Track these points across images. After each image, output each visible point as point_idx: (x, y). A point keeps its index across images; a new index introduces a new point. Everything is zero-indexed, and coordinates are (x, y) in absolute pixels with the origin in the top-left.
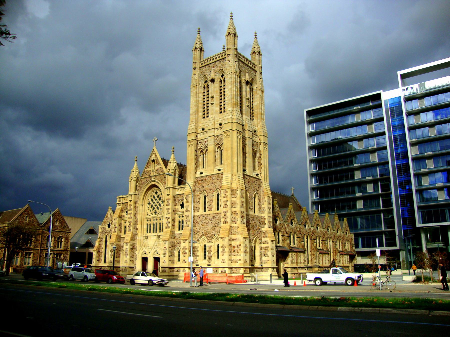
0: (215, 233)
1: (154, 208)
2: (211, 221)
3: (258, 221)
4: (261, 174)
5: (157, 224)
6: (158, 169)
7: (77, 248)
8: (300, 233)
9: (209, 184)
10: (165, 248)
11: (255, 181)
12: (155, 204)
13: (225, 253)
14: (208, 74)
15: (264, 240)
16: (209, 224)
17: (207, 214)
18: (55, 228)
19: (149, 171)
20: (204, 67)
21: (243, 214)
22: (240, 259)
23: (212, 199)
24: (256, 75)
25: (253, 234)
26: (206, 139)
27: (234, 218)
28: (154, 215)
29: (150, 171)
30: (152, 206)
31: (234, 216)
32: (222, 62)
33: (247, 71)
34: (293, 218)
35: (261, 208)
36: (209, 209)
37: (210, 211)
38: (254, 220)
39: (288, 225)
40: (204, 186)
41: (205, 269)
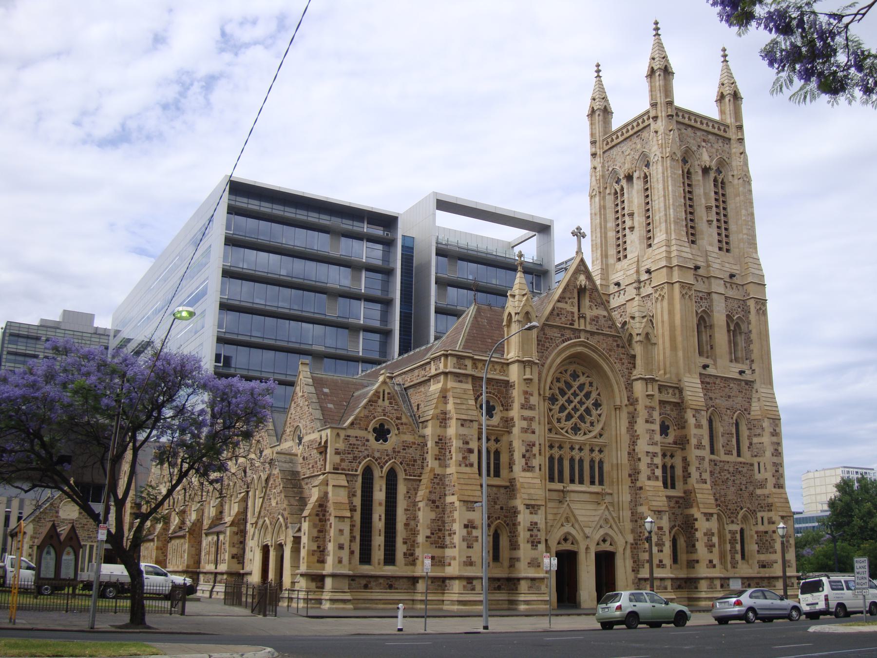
2: (732, 478)
5: (581, 461)
7: (651, 522)
10: (660, 528)
16: (729, 483)
17: (724, 462)
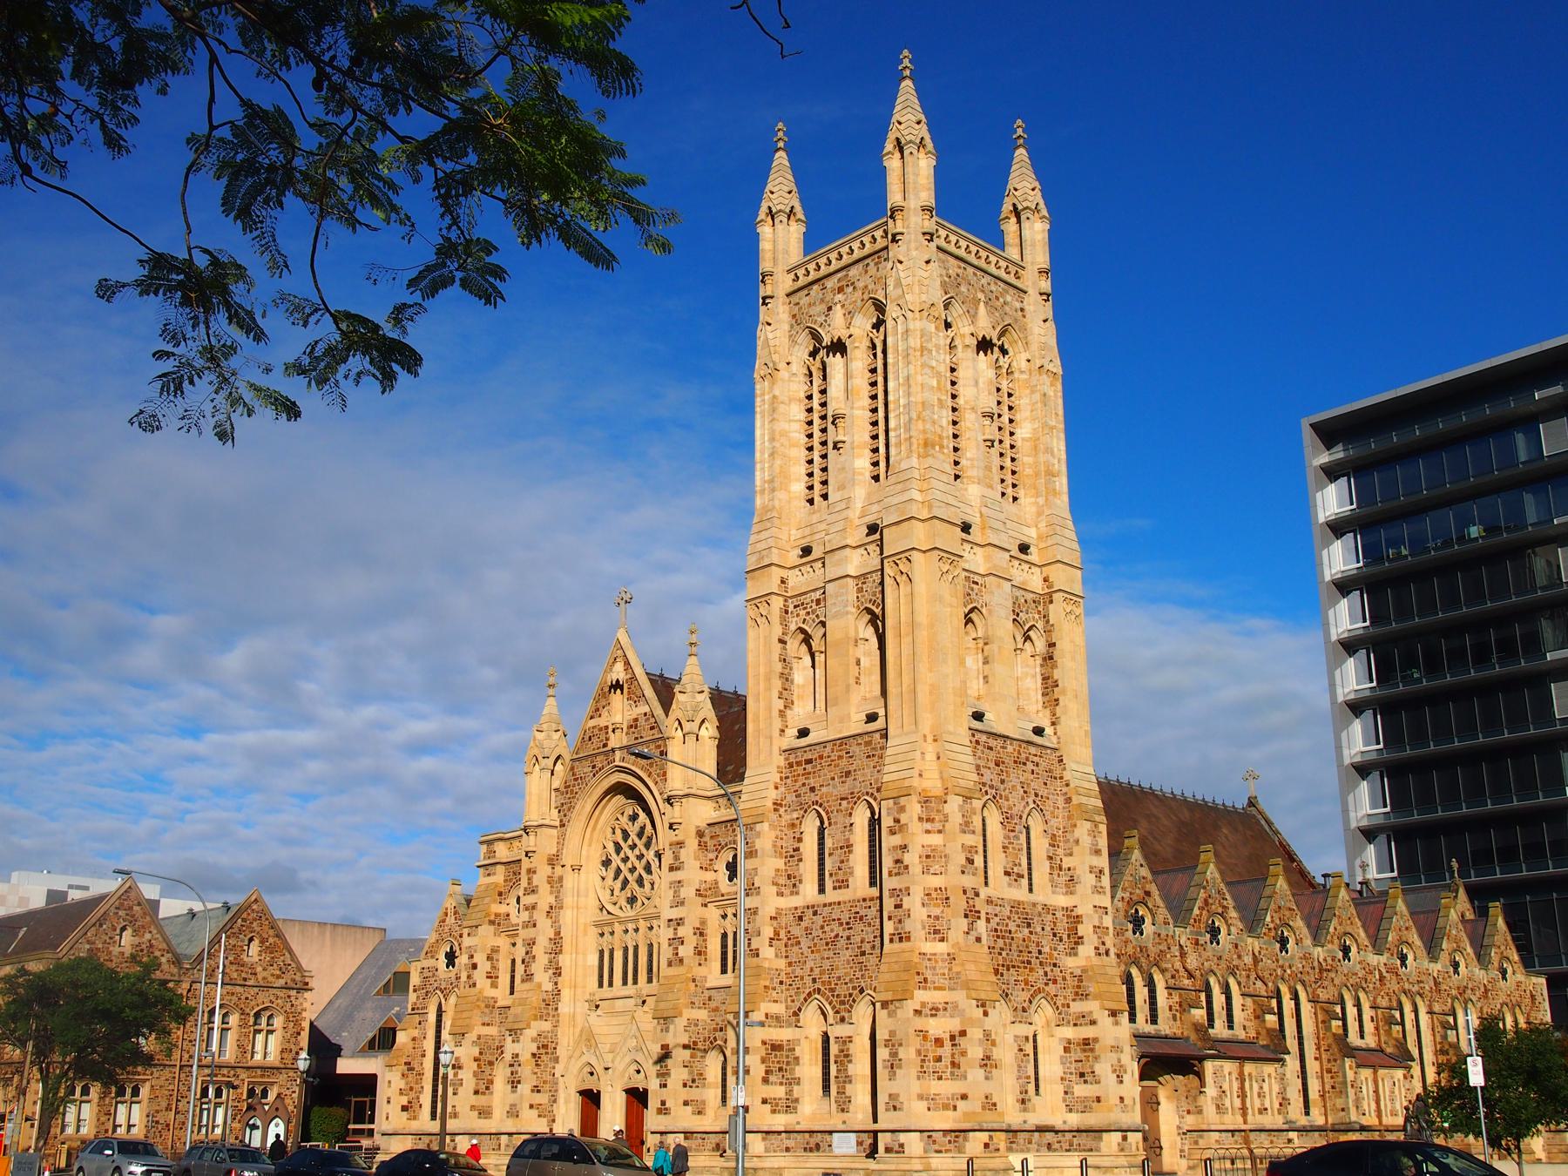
0: (863, 984)
1: (626, 882)
2: (847, 933)
3: (1048, 928)
4: (1058, 727)
6: (636, 720)
8: (1258, 977)
9: (833, 779)
11: (1027, 759)
12: (629, 865)
13: (900, 1067)
14: (821, 319)
15: (1077, 1007)
17: (830, 904)
18: (244, 975)
19: (601, 729)
20: (806, 292)
21: (971, 902)
22: (964, 1091)
23: (848, 840)
24: (1022, 310)
25: (1026, 984)
26: (818, 593)
27: (937, 918)
28: (630, 913)
29: (607, 727)
30: (618, 871)
31: (936, 911)
32: (872, 269)
34: (1220, 910)
35: (1061, 869)
36: (838, 881)
37: (843, 891)
38: (1029, 925)
39: (1197, 943)
40: (817, 786)
41: (827, 1136)
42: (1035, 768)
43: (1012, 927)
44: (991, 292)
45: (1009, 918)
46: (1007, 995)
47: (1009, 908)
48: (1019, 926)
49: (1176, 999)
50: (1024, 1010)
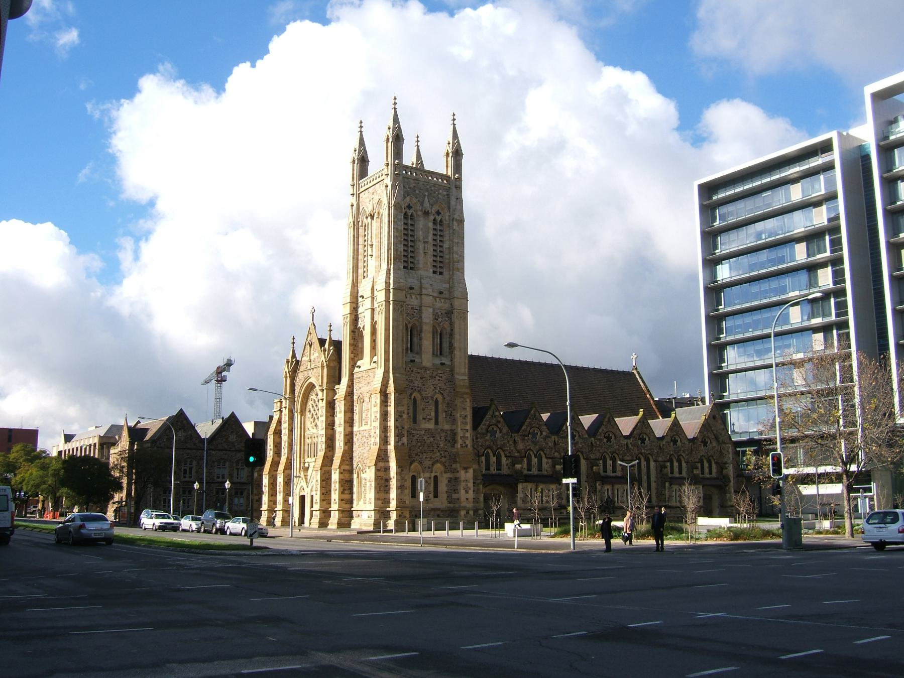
1: (314, 419)
3: (443, 438)
33: (426, 194)
34: (537, 426)
42: (440, 378)
43: (425, 438)
44: (432, 190)
45: (424, 435)
46: (421, 463)
47: (424, 431)
48: (428, 438)
49: (510, 460)
50: (429, 468)
